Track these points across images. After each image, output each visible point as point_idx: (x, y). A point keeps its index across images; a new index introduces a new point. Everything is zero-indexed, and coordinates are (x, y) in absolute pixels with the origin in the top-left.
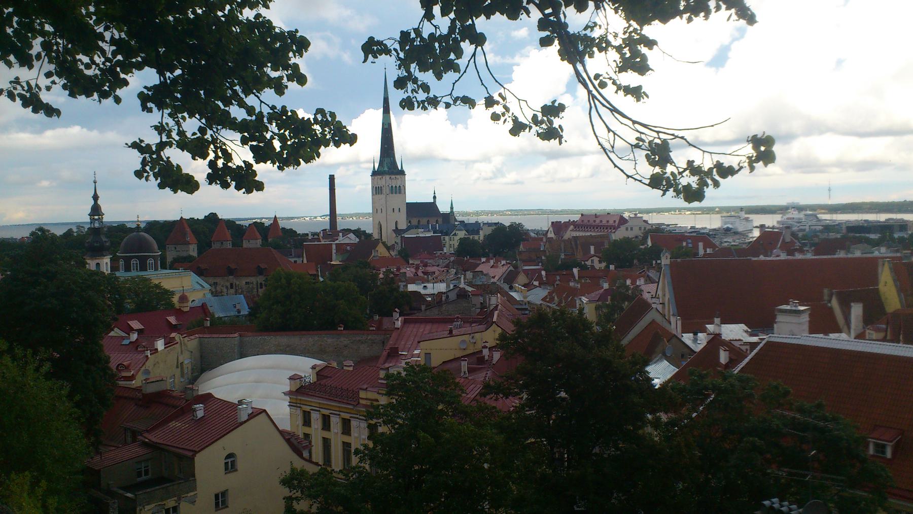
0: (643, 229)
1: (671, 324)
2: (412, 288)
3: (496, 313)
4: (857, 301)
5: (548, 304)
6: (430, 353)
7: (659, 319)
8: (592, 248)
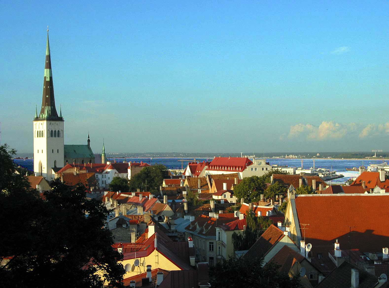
0: (265, 169)
5: (191, 232)
8: (225, 185)
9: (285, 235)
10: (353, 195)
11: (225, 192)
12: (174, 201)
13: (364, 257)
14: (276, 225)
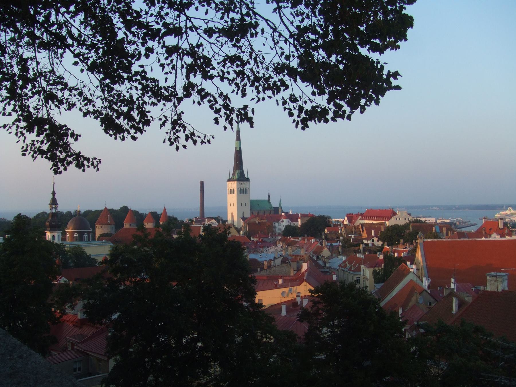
0: (407, 219)
1: (422, 281)
2: (252, 256)
5: (343, 269)
6: (262, 300)
7: (415, 279)
8: (373, 232)
9: (411, 272)
10: (470, 239)
11: (373, 237)
12: (331, 244)
13: (475, 290)
14: (407, 264)
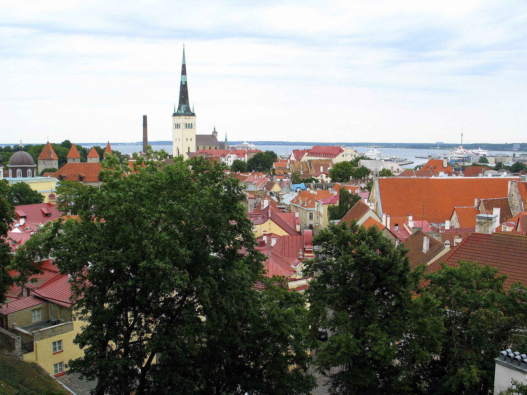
0: (353, 156)
3: (269, 211)
4: (497, 207)
8: (322, 168)
12: (281, 180)
